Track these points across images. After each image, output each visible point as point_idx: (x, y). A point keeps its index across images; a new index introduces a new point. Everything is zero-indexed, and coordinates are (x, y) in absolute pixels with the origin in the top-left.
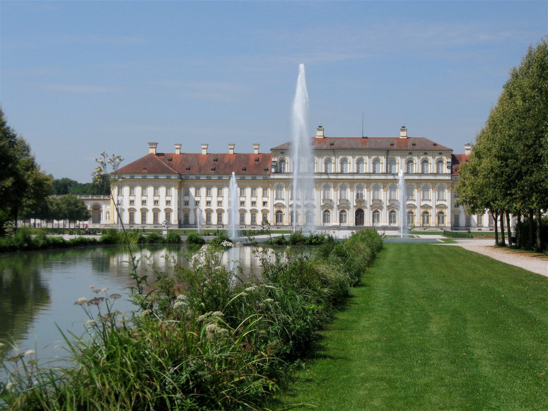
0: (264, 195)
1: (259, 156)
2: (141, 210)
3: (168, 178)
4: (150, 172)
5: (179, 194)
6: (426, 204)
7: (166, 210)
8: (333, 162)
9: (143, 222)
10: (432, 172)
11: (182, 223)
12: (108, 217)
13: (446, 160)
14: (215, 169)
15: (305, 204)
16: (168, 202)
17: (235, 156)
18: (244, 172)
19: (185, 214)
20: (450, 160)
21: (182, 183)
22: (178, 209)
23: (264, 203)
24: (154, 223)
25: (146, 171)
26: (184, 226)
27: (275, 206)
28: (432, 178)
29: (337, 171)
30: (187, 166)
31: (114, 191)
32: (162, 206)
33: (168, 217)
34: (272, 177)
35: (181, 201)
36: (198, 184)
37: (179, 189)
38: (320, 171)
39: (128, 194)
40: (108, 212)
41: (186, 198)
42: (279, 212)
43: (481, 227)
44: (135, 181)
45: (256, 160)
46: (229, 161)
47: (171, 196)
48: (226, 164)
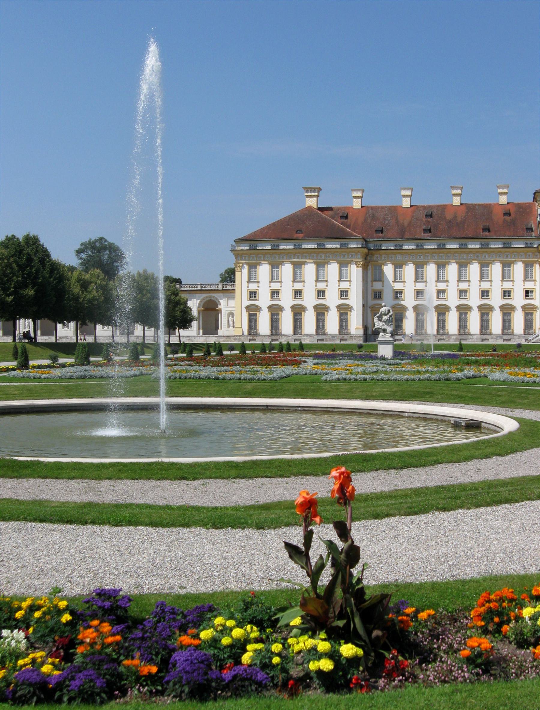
1: (509, 207)
2: (293, 307)
3: (344, 247)
4: (309, 238)
7: (339, 307)
9: (297, 331)
12: (231, 323)
14: (430, 231)
16: (344, 293)
17: (463, 208)
18: (487, 233)
21: (369, 258)
22: (363, 306)
23: (527, 293)
24: (317, 334)
25: (301, 235)
26: (372, 337)
30: (378, 226)
31: (242, 275)
33: (343, 321)
36: (399, 259)
37: (365, 268)
39: (268, 278)
40: (231, 314)
41: (377, 286)
44: (281, 253)
45: (505, 214)
46: (455, 218)
47: (350, 281)
48: (450, 221)
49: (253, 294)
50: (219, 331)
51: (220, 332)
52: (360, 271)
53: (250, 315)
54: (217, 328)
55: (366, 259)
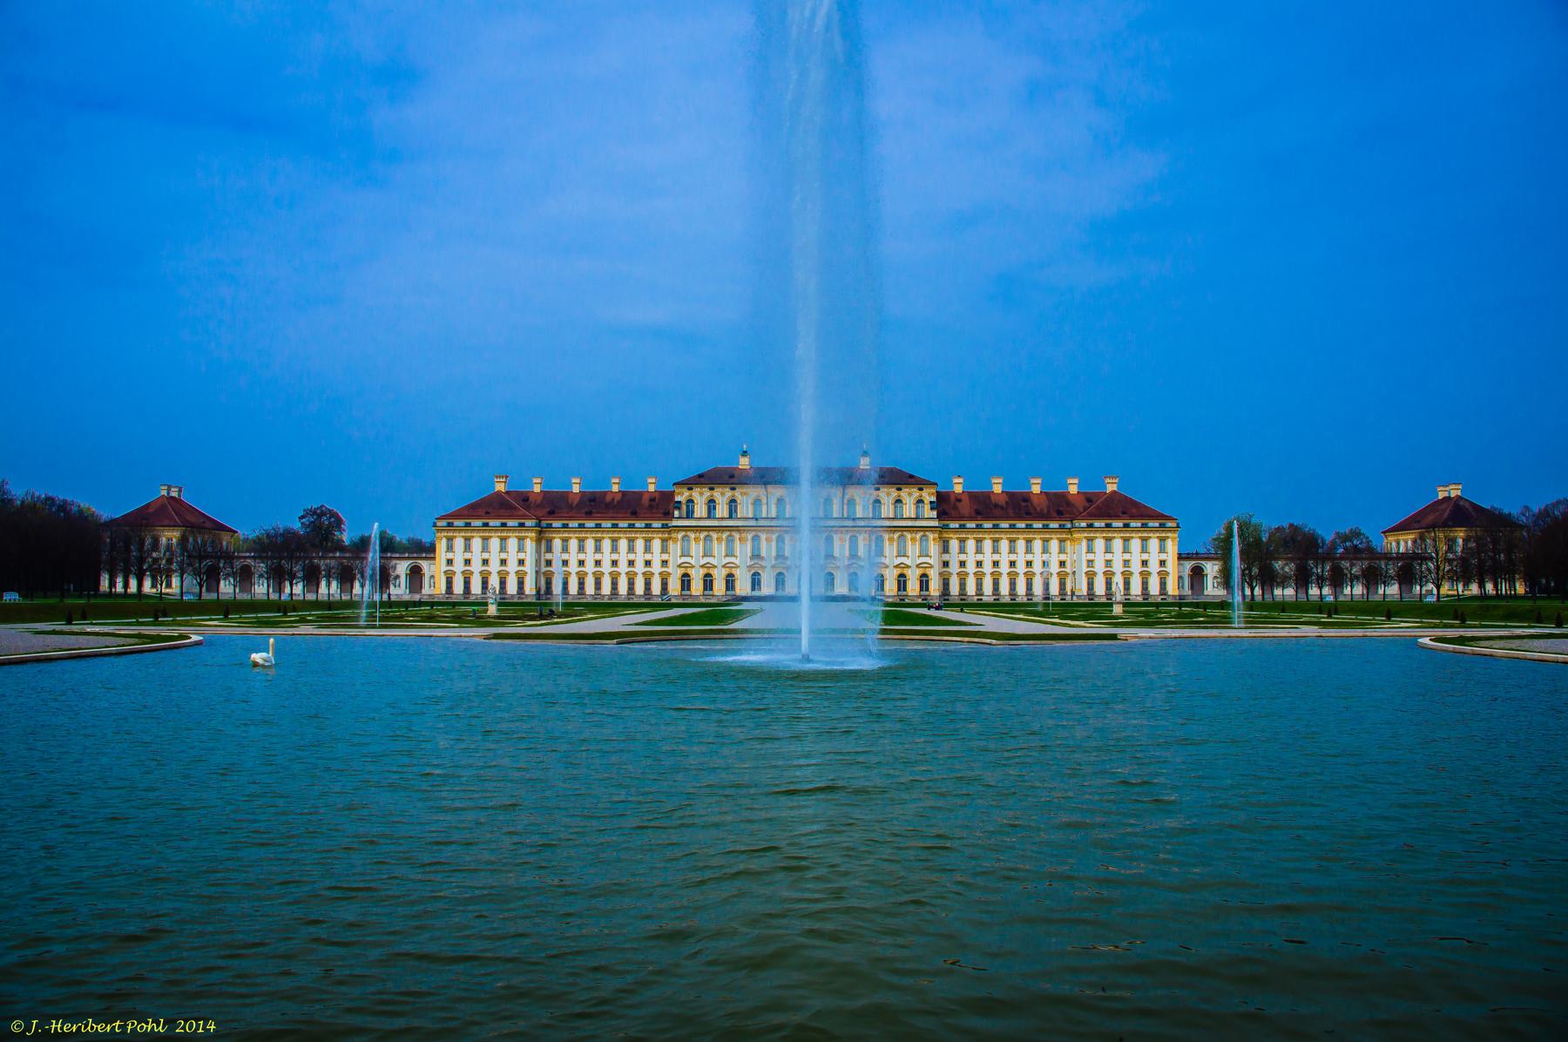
0: (664, 550)
1: (657, 494)
5: (538, 551)
6: (902, 563)
8: (764, 501)
10: (908, 516)
11: (542, 592)
12: (432, 584)
13: (929, 496)
15: (723, 564)
16: (521, 562)
19: (547, 579)
20: (933, 499)
21: (542, 535)
22: (537, 572)
27: (679, 566)
28: (910, 523)
29: (769, 516)
31: (441, 546)
32: (512, 567)
33: (521, 584)
34: (675, 523)
35: (540, 559)
37: (538, 541)
38: (745, 515)
40: (432, 577)
41: (549, 556)
42: (686, 575)
43: (982, 595)
49: (450, 562)
50: (423, 590)
51: (424, 592)
52: (534, 543)
53: (447, 578)
54: (421, 588)
55: (540, 534)
